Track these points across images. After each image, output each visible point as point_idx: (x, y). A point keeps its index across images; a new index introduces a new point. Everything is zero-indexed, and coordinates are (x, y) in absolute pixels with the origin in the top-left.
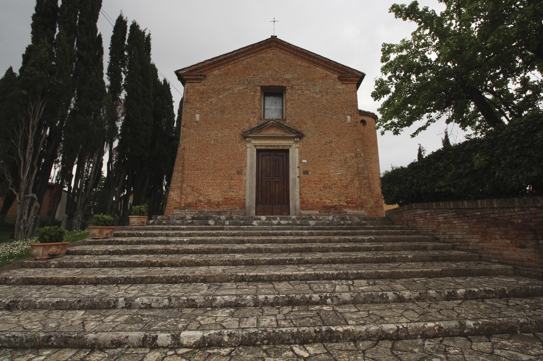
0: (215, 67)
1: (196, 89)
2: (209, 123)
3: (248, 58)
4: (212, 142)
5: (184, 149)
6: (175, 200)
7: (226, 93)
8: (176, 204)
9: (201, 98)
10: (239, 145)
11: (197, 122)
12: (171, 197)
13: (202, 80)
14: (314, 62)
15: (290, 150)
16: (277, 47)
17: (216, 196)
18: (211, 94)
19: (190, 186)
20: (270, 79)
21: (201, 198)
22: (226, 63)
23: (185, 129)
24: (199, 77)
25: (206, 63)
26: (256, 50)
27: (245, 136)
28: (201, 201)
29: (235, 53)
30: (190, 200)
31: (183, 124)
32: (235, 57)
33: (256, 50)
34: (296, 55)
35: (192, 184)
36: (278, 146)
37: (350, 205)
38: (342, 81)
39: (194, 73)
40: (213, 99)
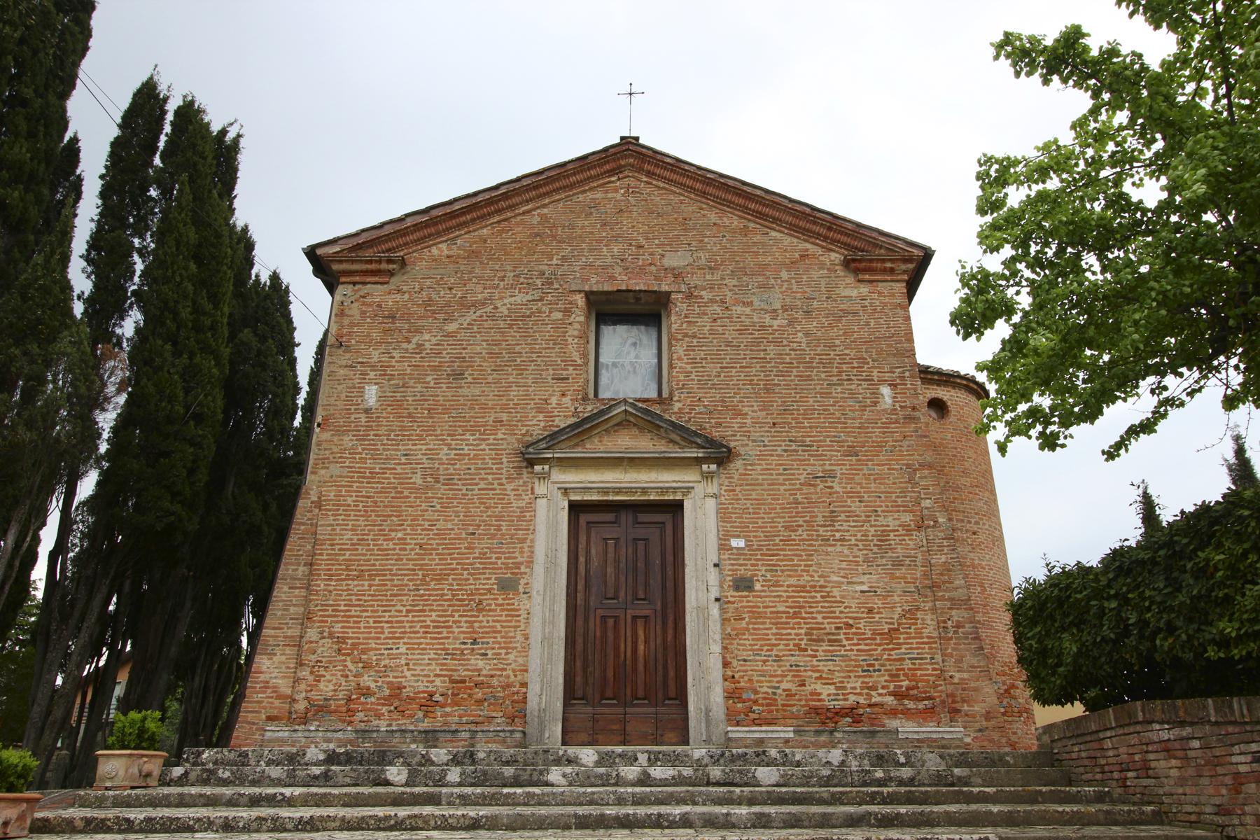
0: (439, 234)
1: (370, 305)
2: (410, 416)
3: (544, 206)
4: (417, 479)
5: (318, 504)
6: (275, 689)
7: (471, 316)
8: (277, 703)
9: (385, 331)
10: (509, 487)
11: (367, 411)
12: (262, 677)
13: (391, 274)
14: (761, 216)
15: (687, 505)
16: (640, 170)
17: (421, 672)
18: (420, 318)
19: (331, 636)
20: (618, 270)
21: (367, 680)
22: (473, 220)
23: (326, 436)
24: (384, 266)
25: (409, 222)
26: (572, 179)
27: (530, 458)
28: (367, 692)
29: (503, 190)
30: (326, 688)
31: (319, 419)
32: (503, 204)
33: (572, 179)
34: (704, 194)
35: (337, 628)
36: (644, 491)
37: (910, 704)
38: (856, 271)
39: (368, 253)
40: (427, 337)
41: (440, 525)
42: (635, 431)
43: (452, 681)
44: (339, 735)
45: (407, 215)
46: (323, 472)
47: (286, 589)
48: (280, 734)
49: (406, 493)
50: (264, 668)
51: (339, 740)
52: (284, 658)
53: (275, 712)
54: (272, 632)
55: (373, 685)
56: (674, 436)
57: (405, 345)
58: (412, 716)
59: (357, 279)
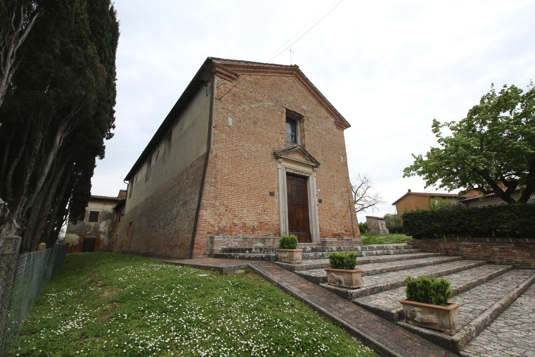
0: (247, 72)
1: (227, 88)
2: (242, 132)
3: (274, 76)
4: (246, 155)
5: (216, 156)
6: (209, 222)
7: (258, 104)
8: (210, 227)
9: (233, 100)
10: (271, 164)
11: (229, 127)
12: (204, 218)
13: (234, 79)
14: (320, 102)
15: (310, 178)
16: (297, 76)
17: (251, 220)
18: (243, 99)
19: (223, 205)
20: (293, 105)
21: (236, 221)
22: (257, 72)
23: (216, 132)
24: (233, 76)
25: (242, 64)
26: (282, 71)
27: (276, 156)
28: (236, 225)
29: (267, 66)
30: (224, 223)
31: (214, 125)
32: (265, 70)
33: (282, 71)
34: (310, 91)
35: (225, 202)
36: (302, 172)
37: (347, 233)
38: (337, 125)
39: (229, 69)
40: (246, 106)
41: (253, 172)
42: (299, 154)
43: (259, 223)
44: (238, 239)
45: (242, 61)
46: (217, 145)
47: (208, 186)
48: (220, 239)
49: (243, 159)
50: (204, 215)
51: (238, 241)
52: (210, 211)
53: (210, 231)
54: (206, 202)
55: (237, 223)
56: (308, 158)
57: (239, 107)
58: (249, 233)
59: (223, 76)
